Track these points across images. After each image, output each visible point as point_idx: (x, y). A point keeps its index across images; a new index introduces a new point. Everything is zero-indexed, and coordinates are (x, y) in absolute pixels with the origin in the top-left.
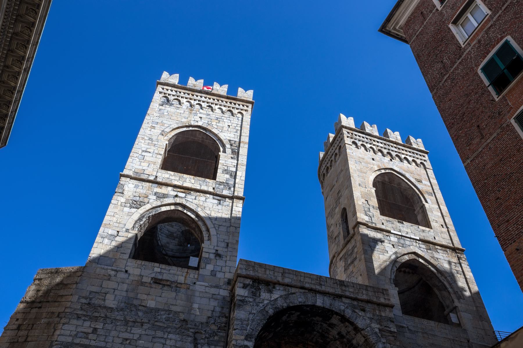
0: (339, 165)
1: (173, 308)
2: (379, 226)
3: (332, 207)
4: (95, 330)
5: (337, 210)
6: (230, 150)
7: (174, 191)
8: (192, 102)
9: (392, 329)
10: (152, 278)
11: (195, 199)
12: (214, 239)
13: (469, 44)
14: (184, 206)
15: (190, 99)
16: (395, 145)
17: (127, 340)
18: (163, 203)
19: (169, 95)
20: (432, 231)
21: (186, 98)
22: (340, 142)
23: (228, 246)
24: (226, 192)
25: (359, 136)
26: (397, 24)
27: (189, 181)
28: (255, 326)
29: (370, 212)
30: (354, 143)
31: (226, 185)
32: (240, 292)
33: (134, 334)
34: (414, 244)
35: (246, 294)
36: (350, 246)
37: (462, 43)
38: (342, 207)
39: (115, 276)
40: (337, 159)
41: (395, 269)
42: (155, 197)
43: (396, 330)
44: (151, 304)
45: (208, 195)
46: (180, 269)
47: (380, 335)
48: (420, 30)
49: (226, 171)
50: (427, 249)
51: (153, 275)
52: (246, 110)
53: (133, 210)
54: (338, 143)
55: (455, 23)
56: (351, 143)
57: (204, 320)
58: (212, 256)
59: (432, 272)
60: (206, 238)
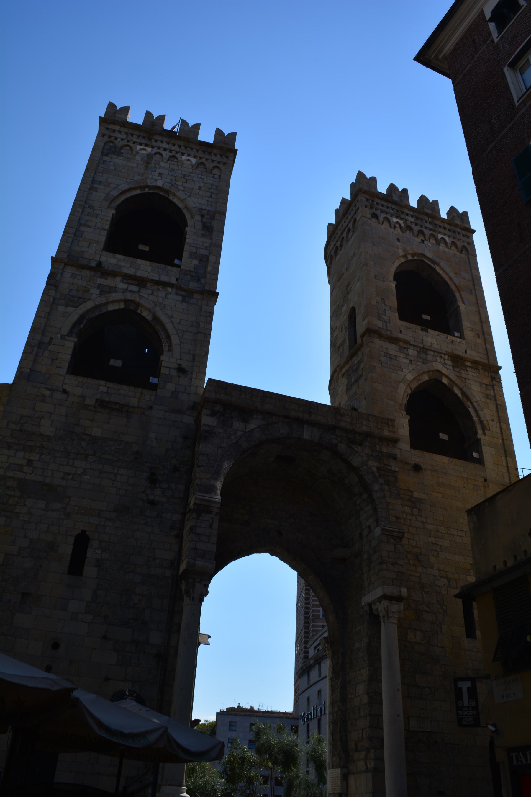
4: (30, 462)
5: (344, 308)
7: (123, 282)
8: (149, 150)
9: (393, 468)
10: (97, 400)
13: (523, 102)
14: (138, 305)
15: (146, 145)
16: (430, 220)
17: (69, 474)
18: (109, 300)
19: (116, 138)
20: (464, 342)
21: (141, 144)
22: (355, 213)
23: (194, 359)
24: (193, 285)
25: (383, 206)
26: (440, 51)
27: (145, 268)
29: (385, 315)
30: (375, 216)
32: (207, 420)
33: (77, 467)
34: (438, 359)
35: (215, 424)
36: (355, 360)
37: (516, 100)
38: (351, 306)
40: (349, 237)
41: (409, 392)
42: (98, 292)
43: (397, 469)
44: (97, 432)
45: (169, 289)
47: (377, 475)
48: (469, 67)
49: (193, 255)
50: (453, 367)
52: (224, 164)
53: (70, 309)
54: (353, 213)
55: (512, 66)
56: (369, 216)
58: (174, 373)
59: (456, 395)
60: (166, 348)
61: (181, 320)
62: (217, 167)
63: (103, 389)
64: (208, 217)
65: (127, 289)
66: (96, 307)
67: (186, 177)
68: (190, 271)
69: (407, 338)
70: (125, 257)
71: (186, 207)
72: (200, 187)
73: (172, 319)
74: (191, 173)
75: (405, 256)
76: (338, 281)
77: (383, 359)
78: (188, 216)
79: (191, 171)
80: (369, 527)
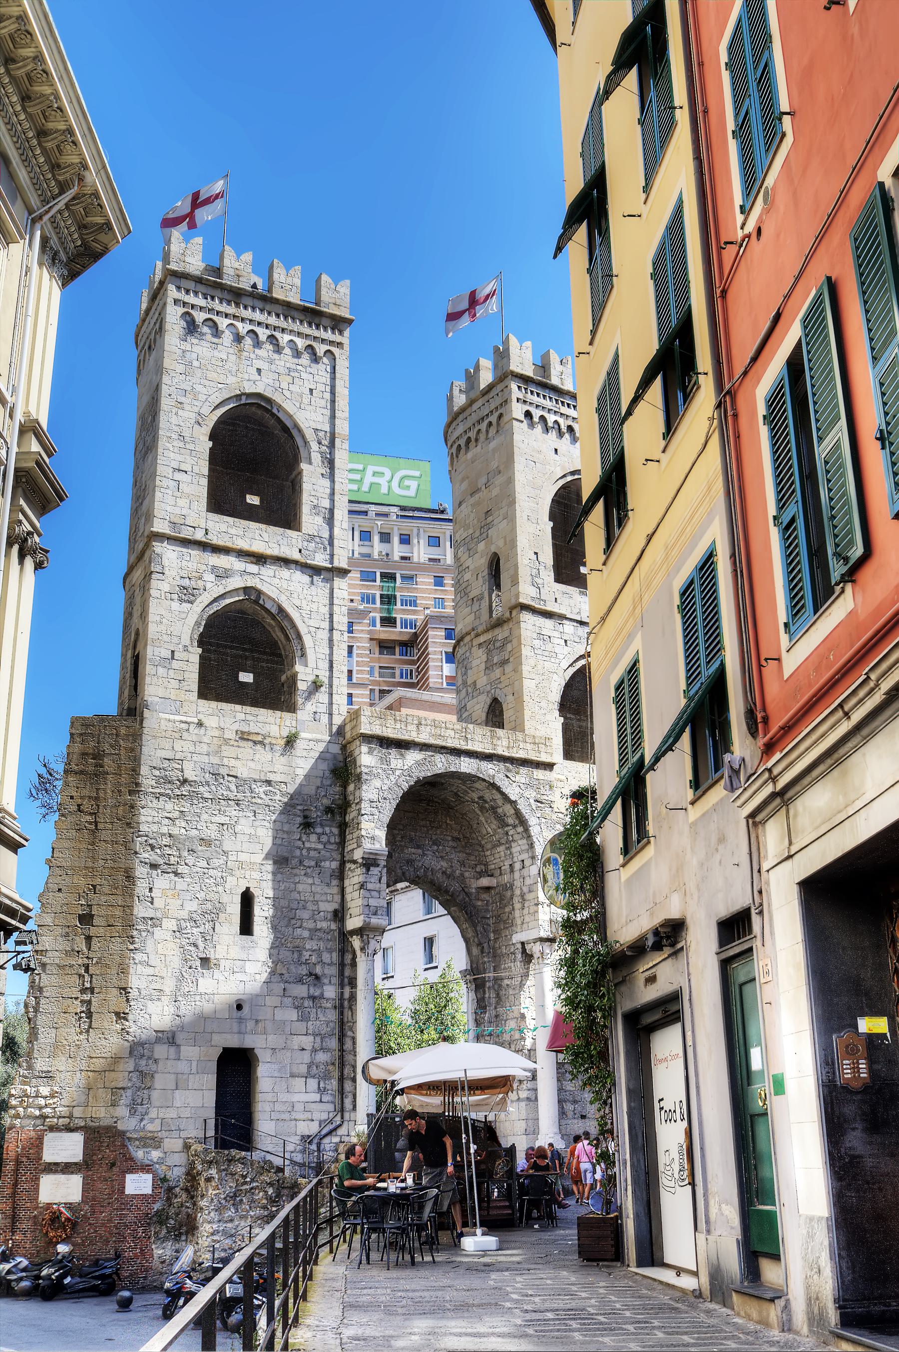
0: (494, 450)
1: (271, 777)
2: (550, 607)
3: (471, 531)
8: (239, 325)
14: (259, 593)
15: (235, 317)
18: (227, 590)
19: (193, 306)
21: (227, 316)
24: (320, 560)
28: (388, 811)
31: (318, 540)
38: (493, 549)
39: (188, 730)
44: (243, 772)
46: (270, 712)
51: (236, 727)
54: (498, 401)
56: (522, 417)
57: (313, 792)
63: (242, 716)
66: (215, 600)
69: (562, 611)
70: (236, 520)
72: (311, 390)
75: (564, 476)
76: (472, 495)
77: (537, 643)
80: (523, 861)
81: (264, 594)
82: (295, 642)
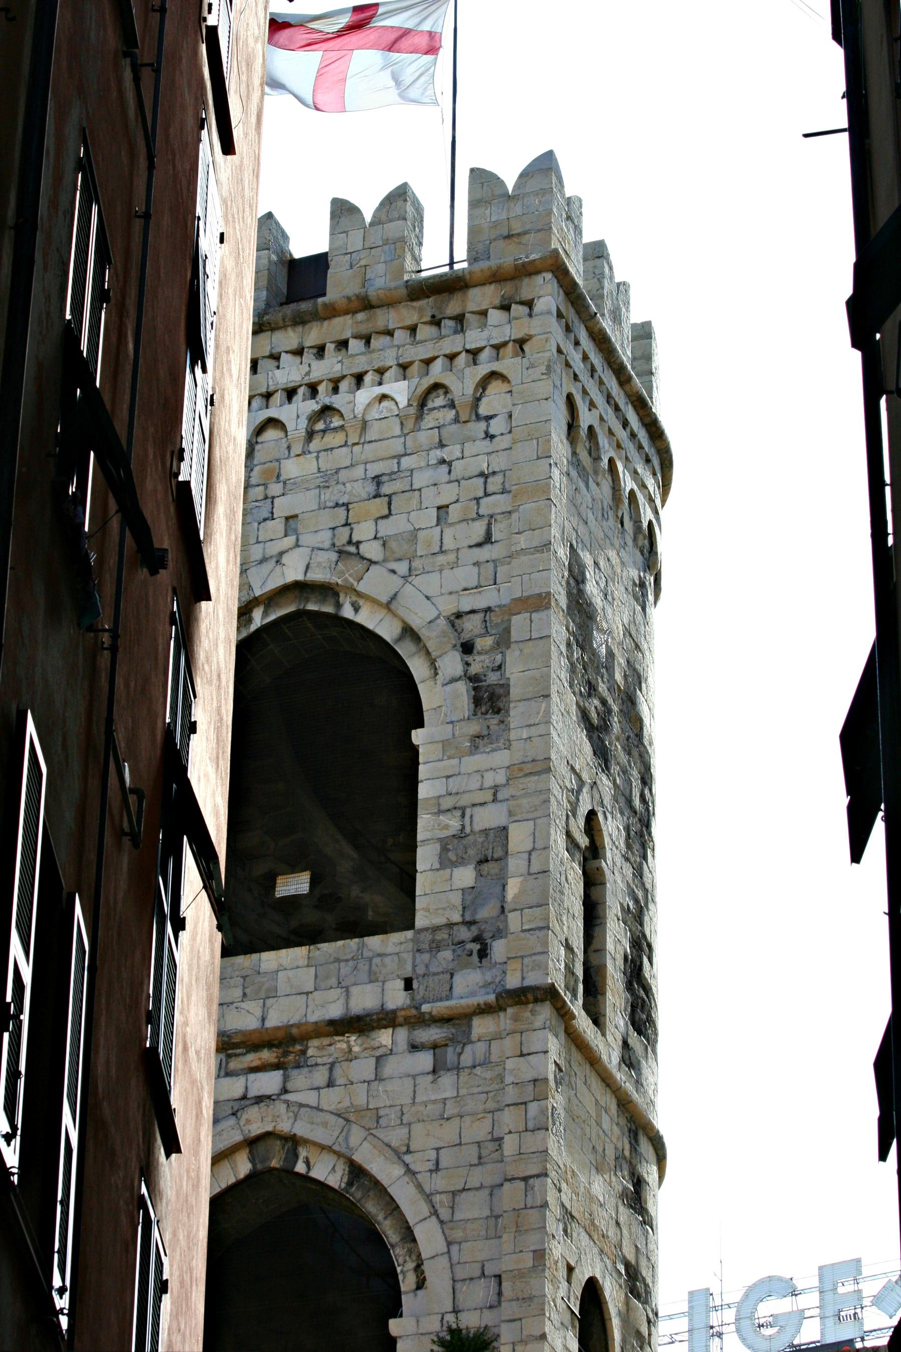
6: (463, 689)
11: (330, 1084)
12: (438, 1275)
14: (293, 1142)
23: (500, 1294)
31: (464, 934)
45: (384, 1037)
49: (452, 851)
60: (407, 1282)
61: (438, 1149)
62: (493, 375)
64: (489, 641)
65: (244, 1097)
67: (386, 489)
68: (450, 925)
71: (409, 632)
73: (408, 1158)
74: (399, 457)
78: (418, 668)
79: (397, 446)
81: (306, 1142)
82: (399, 1254)
